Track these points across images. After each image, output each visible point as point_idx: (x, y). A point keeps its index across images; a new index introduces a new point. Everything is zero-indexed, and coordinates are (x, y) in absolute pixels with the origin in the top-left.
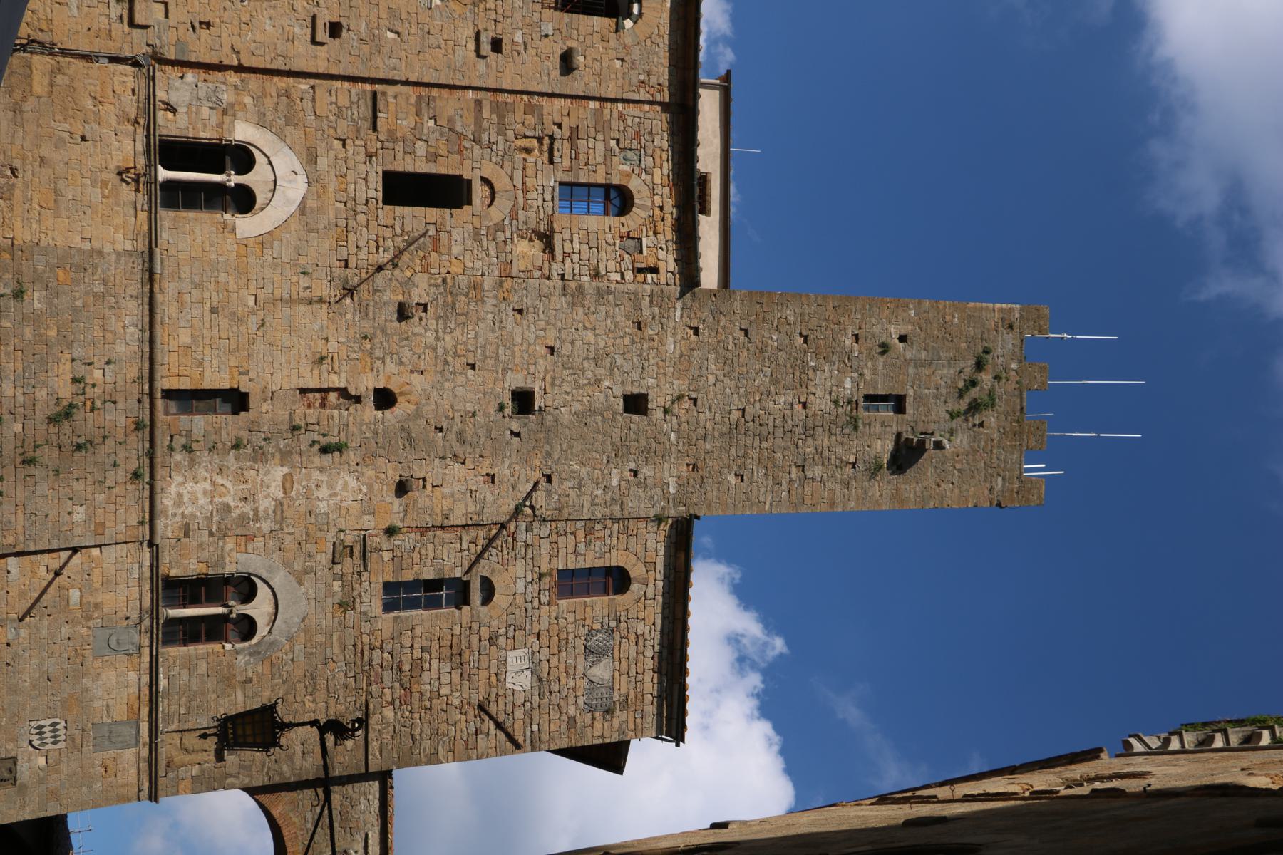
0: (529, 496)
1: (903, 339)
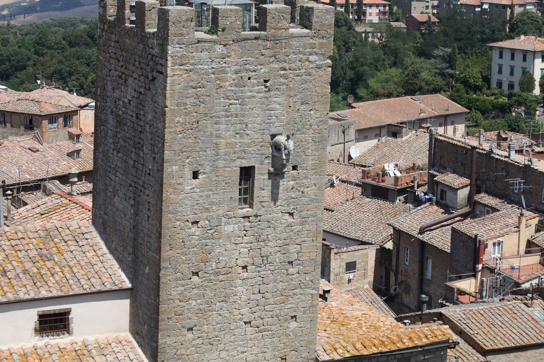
1: (195, 175)
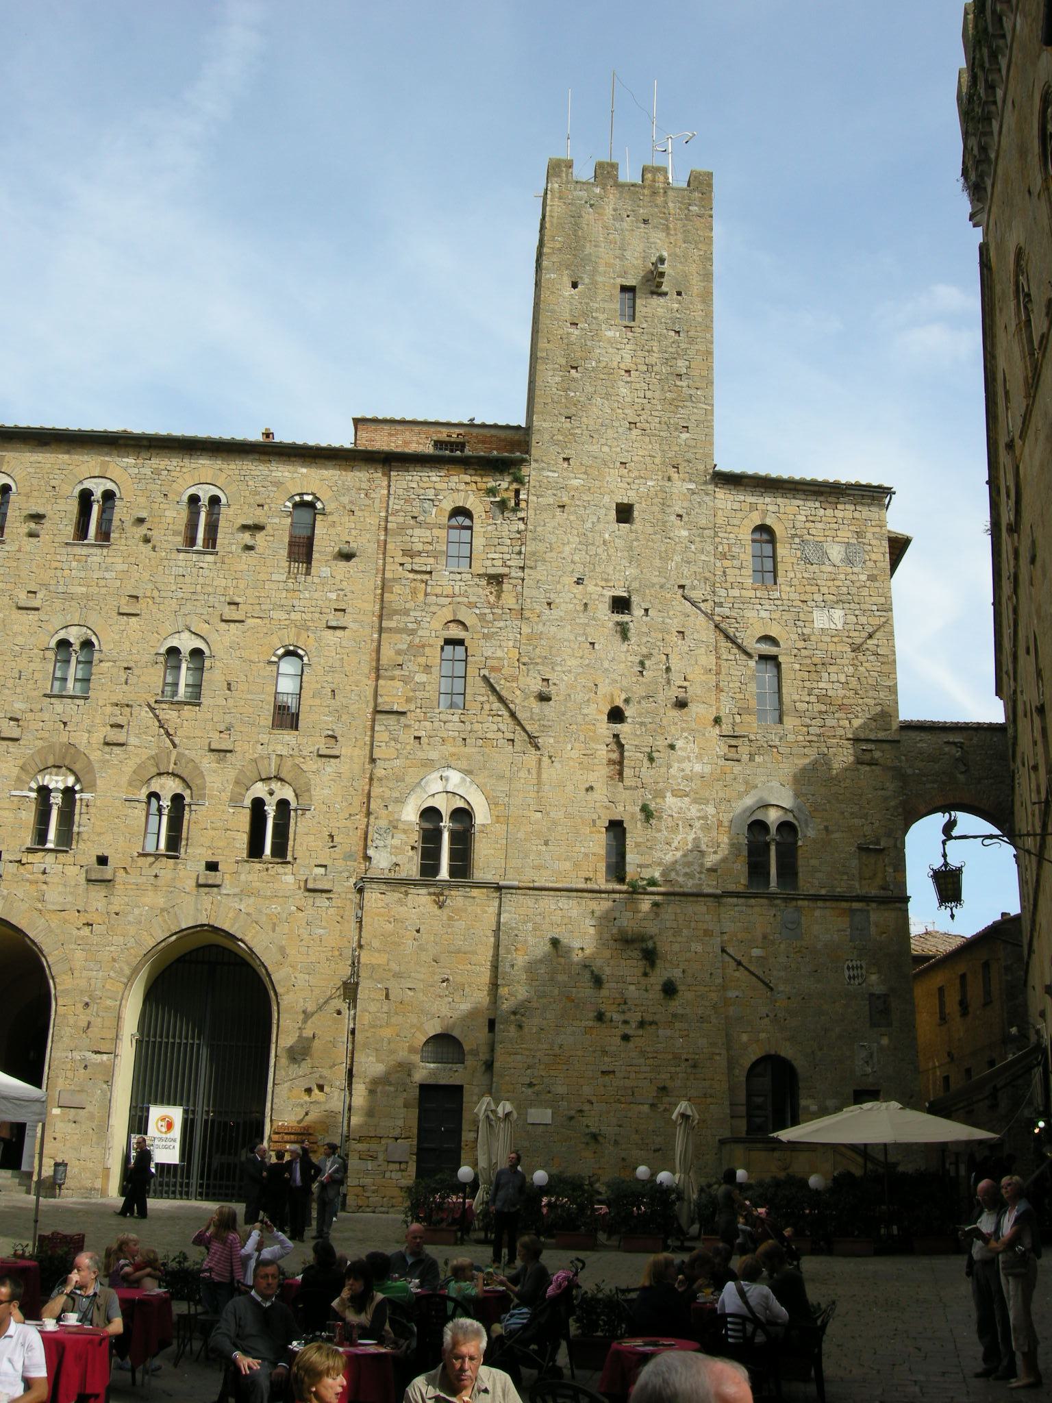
0: (693, 604)
